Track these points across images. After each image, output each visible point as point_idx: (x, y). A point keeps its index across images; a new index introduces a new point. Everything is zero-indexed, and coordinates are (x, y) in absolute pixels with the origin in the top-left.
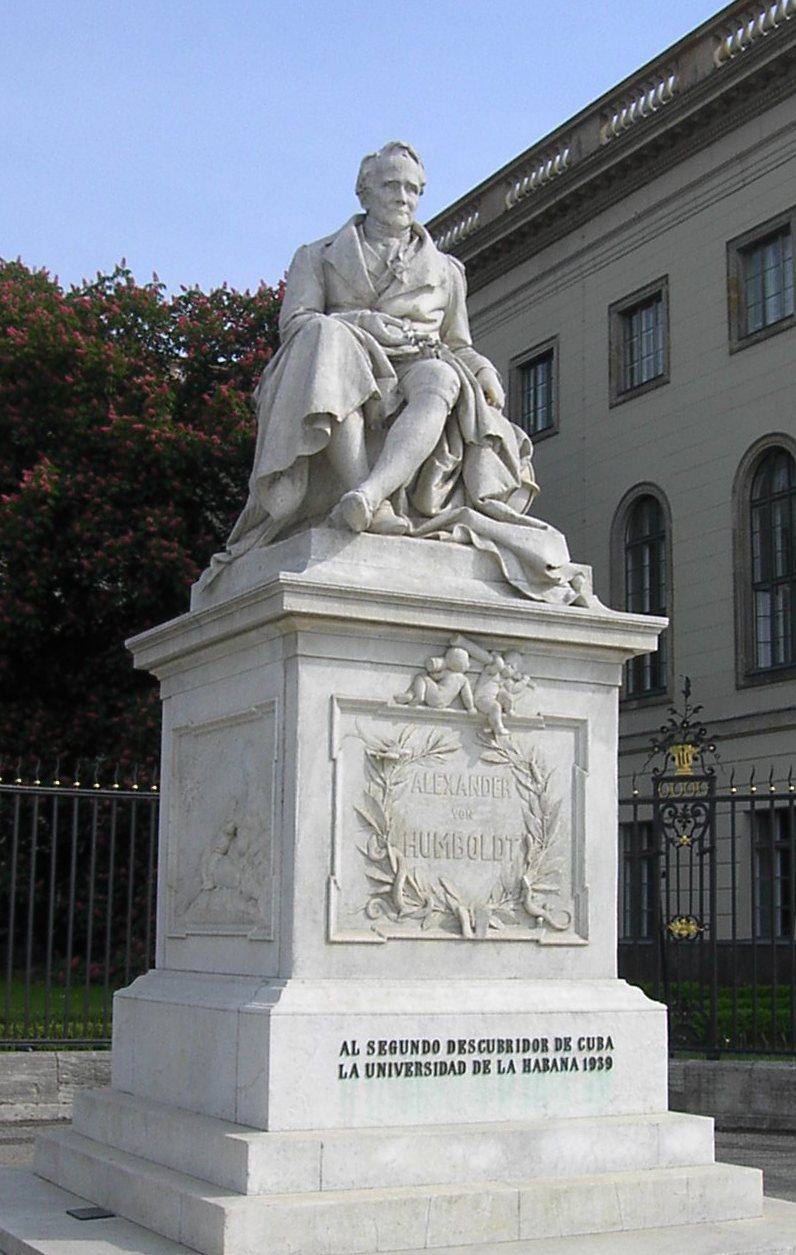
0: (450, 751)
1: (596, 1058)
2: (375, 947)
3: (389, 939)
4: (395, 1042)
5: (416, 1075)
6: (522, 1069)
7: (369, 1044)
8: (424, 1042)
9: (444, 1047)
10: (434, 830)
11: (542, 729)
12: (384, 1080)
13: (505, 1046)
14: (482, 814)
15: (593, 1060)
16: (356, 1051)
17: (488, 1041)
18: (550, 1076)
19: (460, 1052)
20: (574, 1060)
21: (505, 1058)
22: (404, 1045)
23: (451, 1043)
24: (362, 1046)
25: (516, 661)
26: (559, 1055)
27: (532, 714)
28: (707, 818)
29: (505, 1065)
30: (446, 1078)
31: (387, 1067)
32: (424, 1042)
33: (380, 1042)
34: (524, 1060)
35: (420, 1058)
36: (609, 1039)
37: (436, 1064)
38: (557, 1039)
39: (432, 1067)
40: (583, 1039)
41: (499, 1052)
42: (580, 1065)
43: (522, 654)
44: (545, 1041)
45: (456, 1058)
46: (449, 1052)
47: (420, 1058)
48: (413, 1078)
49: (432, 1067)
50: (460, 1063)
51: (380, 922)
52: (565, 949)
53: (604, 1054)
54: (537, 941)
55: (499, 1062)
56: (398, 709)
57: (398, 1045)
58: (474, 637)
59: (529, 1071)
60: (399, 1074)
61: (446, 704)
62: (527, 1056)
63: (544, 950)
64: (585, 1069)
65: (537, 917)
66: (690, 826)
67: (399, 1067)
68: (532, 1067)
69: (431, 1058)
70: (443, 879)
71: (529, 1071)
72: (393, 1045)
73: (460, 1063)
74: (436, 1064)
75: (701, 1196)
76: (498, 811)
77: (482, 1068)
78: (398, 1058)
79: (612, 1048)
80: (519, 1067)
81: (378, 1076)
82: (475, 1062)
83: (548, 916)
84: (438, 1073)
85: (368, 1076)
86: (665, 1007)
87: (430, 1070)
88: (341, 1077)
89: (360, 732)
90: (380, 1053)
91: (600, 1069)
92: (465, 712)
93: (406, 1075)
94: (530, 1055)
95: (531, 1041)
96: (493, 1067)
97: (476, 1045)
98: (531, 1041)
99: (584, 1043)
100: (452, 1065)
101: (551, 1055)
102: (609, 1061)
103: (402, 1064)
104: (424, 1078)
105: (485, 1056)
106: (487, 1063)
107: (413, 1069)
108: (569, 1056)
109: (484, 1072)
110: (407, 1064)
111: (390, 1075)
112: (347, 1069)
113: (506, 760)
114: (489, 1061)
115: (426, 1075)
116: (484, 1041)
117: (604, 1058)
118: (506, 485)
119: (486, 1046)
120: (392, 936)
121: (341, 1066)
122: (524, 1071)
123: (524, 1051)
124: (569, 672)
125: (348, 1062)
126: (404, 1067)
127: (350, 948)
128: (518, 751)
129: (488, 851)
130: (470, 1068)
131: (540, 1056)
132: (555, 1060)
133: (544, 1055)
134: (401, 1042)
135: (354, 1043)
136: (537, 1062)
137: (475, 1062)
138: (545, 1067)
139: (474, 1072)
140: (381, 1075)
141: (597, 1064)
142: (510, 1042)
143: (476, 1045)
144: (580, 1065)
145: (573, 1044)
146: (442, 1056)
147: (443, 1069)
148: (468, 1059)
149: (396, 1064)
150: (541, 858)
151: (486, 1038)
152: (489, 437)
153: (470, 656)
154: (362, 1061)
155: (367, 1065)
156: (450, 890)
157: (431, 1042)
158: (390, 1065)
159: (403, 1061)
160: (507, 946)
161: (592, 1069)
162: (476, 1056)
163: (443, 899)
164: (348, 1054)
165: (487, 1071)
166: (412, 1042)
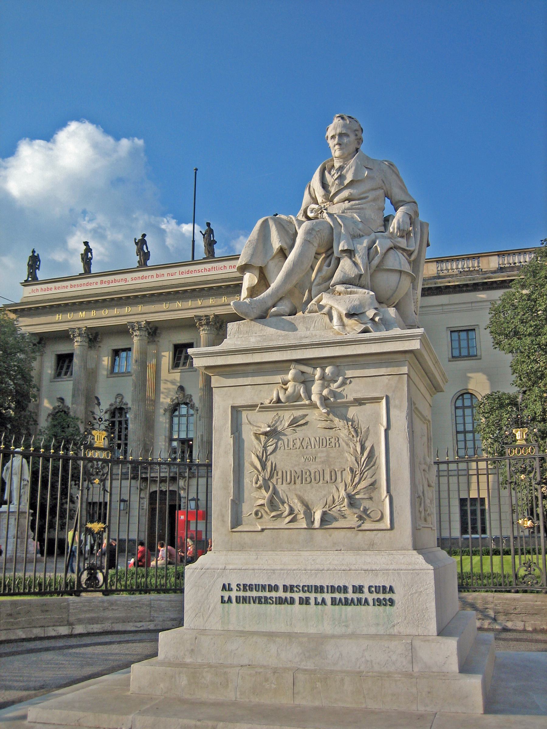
1: (382, 598)
4: (252, 585)
7: (237, 585)
9: (281, 588)
12: (247, 605)
13: (320, 589)
14: (320, 458)
15: (378, 599)
16: (230, 589)
17: (308, 586)
21: (320, 597)
24: (234, 587)
26: (355, 596)
29: (320, 600)
31: (248, 598)
32: (269, 585)
33: (244, 585)
34: (332, 598)
35: (268, 594)
36: (391, 587)
37: (276, 598)
38: (353, 586)
40: (372, 586)
42: (371, 602)
45: (288, 595)
46: (284, 592)
47: (268, 594)
48: (263, 606)
49: (274, 600)
50: (291, 598)
51: (260, 520)
53: (388, 596)
58: (305, 362)
62: (334, 595)
64: (374, 605)
71: (335, 605)
75: (429, 693)
76: (331, 455)
77: (305, 602)
78: (254, 594)
79: (393, 592)
80: (329, 601)
81: (243, 603)
82: (300, 598)
86: (432, 567)
88: (222, 602)
94: (337, 595)
96: (312, 601)
99: (373, 589)
101: (350, 595)
102: (392, 602)
104: (269, 605)
105: (307, 595)
106: (308, 599)
107: (263, 600)
108: (363, 596)
110: (259, 597)
111: (249, 603)
112: (226, 599)
116: (305, 586)
120: (264, 527)
122: (332, 604)
125: (226, 595)
129: (327, 477)
131: (342, 596)
135: (229, 584)
137: (300, 598)
138: (347, 602)
139: (300, 604)
142: (322, 587)
143: (301, 588)
144: (371, 602)
145: (366, 590)
146: (281, 594)
147: (281, 601)
148: (296, 596)
150: (357, 480)
154: (234, 594)
155: (236, 597)
157: (273, 585)
159: (258, 595)
160: (336, 532)
166: (262, 585)
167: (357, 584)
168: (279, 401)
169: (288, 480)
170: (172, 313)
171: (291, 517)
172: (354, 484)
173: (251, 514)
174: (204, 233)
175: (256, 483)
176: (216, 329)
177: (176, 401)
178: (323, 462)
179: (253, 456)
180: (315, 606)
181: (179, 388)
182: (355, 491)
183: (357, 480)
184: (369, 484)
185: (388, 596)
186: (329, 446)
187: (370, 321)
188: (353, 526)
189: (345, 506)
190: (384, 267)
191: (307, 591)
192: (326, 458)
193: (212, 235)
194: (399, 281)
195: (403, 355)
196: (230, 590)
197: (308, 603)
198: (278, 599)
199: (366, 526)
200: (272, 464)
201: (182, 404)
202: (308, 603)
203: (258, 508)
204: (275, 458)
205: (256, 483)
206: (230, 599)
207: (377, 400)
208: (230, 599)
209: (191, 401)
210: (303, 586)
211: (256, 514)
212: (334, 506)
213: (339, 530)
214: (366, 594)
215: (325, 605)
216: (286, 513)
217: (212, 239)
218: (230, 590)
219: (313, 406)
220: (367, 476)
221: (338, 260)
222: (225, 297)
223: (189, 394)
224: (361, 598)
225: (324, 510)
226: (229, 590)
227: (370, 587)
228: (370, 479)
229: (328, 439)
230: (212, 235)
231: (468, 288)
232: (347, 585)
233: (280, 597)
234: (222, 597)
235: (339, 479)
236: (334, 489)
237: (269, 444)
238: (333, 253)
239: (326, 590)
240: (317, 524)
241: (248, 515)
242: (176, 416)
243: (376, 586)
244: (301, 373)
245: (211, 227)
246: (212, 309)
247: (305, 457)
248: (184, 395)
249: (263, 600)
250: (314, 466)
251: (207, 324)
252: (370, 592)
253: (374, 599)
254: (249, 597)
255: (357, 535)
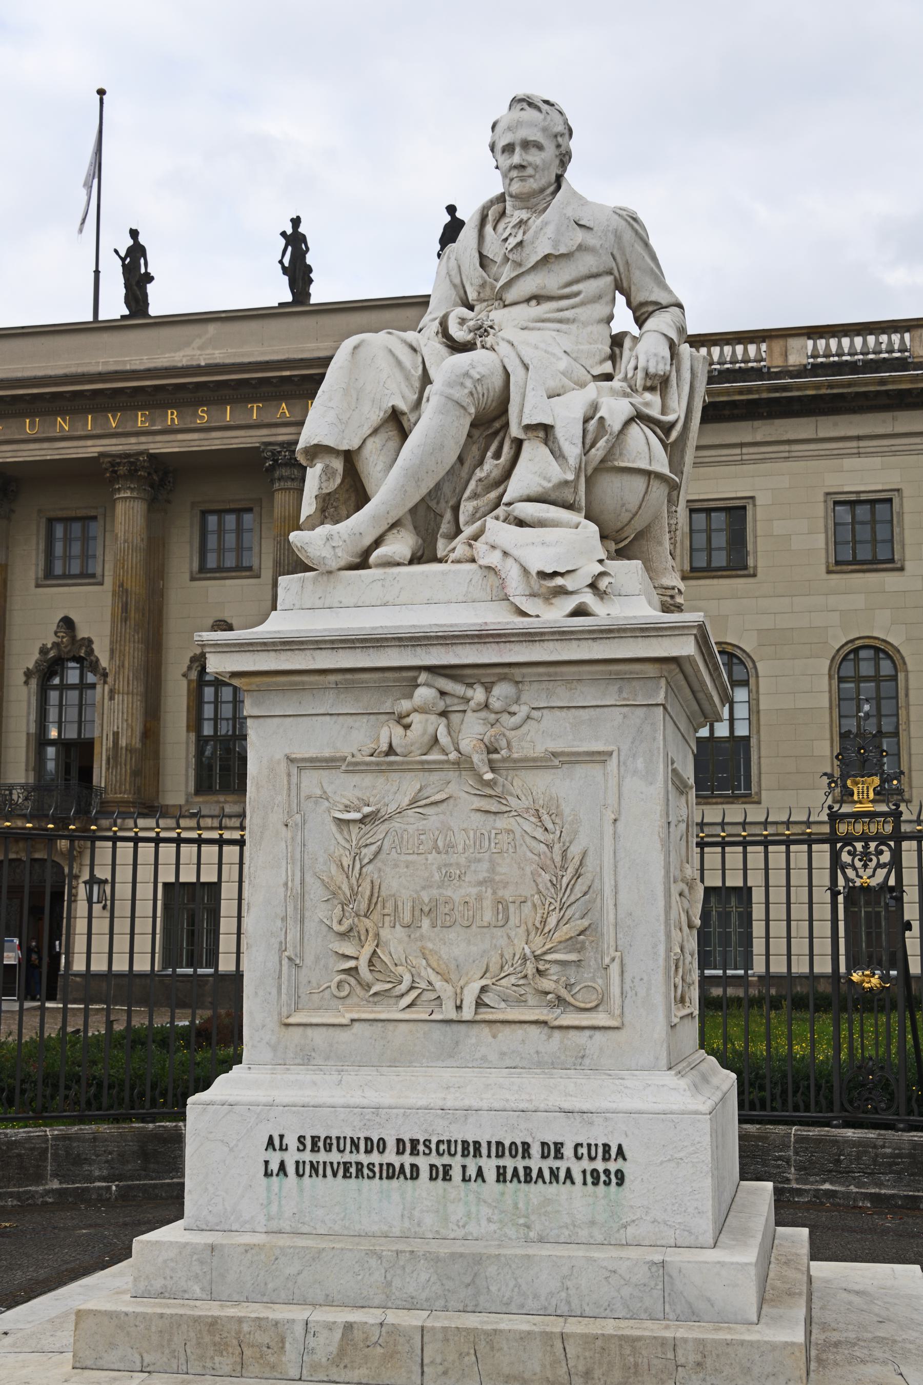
0: (432, 804)
1: (601, 1170)
2: (338, 1031)
3: (353, 1020)
4: (331, 1138)
5: (357, 1177)
6: (494, 1177)
8: (367, 1139)
10: (415, 896)
11: (556, 767)
13: (472, 1149)
16: (284, 1147)
17: (449, 1142)
18: (536, 1191)
19: (412, 1154)
20: (568, 1171)
22: (342, 1141)
23: (399, 1141)
24: (291, 1141)
25: (502, 690)
26: (546, 1165)
27: (539, 750)
28: (892, 856)
29: (472, 1171)
30: (395, 1183)
32: (367, 1139)
33: (313, 1138)
34: (498, 1167)
36: (620, 1147)
38: (543, 1144)
39: (377, 1169)
40: (581, 1145)
41: (463, 1155)
43: (517, 683)
44: (526, 1146)
45: (408, 1159)
46: (398, 1153)
48: (353, 1180)
49: (377, 1169)
50: (413, 1166)
51: (349, 1001)
52: (587, 1033)
53: (613, 1166)
54: (545, 1023)
55: (464, 1167)
56: (367, 764)
57: (334, 1142)
58: (448, 672)
59: (505, 1181)
60: (335, 1175)
61: (419, 752)
62: (501, 1162)
63: (557, 1034)
64: (585, 1183)
65: (547, 993)
66: (873, 864)
67: (335, 1166)
68: (509, 1176)
69: (375, 1158)
70: (427, 952)
72: (328, 1141)
73: (413, 1166)
74: (381, 1165)
78: (335, 1157)
79: (625, 1159)
80: (490, 1174)
81: (311, 1176)
82: (432, 1166)
83: (564, 993)
84: (384, 1175)
85: (299, 1175)
87: (374, 1173)
89: (325, 792)
90: (312, 1150)
91: (607, 1184)
92: (444, 757)
93: (345, 1176)
94: (509, 1163)
95: (507, 1145)
96: (456, 1173)
97: (433, 1146)
98: (507, 1145)
99: (583, 1151)
100: (402, 1166)
101: (535, 1163)
103: (339, 1163)
104: (366, 1180)
105: (446, 1160)
106: (447, 1168)
107: (353, 1170)
108: (562, 1165)
109: (444, 1179)
110: (345, 1163)
111: (325, 1176)
112: (274, 1166)
113: (508, 809)
114: (450, 1166)
115: (369, 1177)
116: (443, 1141)
117: (613, 1171)
118: (549, 481)
119: (447, 1147)
121: (267, 1163)
122: (498, 1181)
123: (497, 1156)
124: (588, 695)
126: (342, 1166)
127: (309, 1031)
128: (523, 798)
129: (488, 916)
130: (424, 1173)
131: (520, 1164)
132: (540, 1170)
133: (527, 1162)
134: (338, 1138)
135: (282, 1137)
136: (515, 1169)
137: (432, 1166)
139: (431, 1179)
140: (314, 1175)
141: (603, 1178)
142: (477, 1144)
143: (433, 1146)
144: (578, 1177)
145: (568, 1151)
146: (391, 1157)
147: (391, 1172)
148: (423, 1163)
149: (331, 1163)
150: (552, 921)
151: (445, 1138)
152: (528, 428)
153: (443, 693)
154: (291, 1158)
155: (297, 1163)
156: (435, 965)
158: (325, 1163)
161: (595, 1183)
162: (434, 1159)
163: (423, 973)
164: (274, 1150)
165: (447, 1177)
166: (352, 1139)
167: (550, 1139)
168: (391, 751)
169: (407, 918)
170: (45, 445)
171: (414, 994)
172: (546, 930)
173: (329, 987)
174: (123, 254)
175: (340, 922)
176: (152, 486)
177: (52, 654)
178: (480, 883)
179: (334, 869)
180: (462, 1185)
181: (61, 623)
182: (547, 946)
183: (552, 921)
184: (578, 932)
185: (613, 1166)
186: (495, 851)
187: (588, 590)
188: (542, 1018)
189: (525, 977)
190: (616, 463)
191: (446, 1152)
192: (486, 875)
193: (142, 261)
194: (646, 493)
195: (657, 666)
196: (283, 1149)
197: (448, 1178)
198: (385, 1167)
199: (570, 1019)
200: (372, 882)
201: (69, 660)
202: (448, 1178)
203: (343, 976)
204: (380, 870)
205: (340, 922)
206: (282, 1167)
207: (600, 757)
208: (282, 1167)
209: (91, 652)
210: (439, 1142)
211: (339, 985)
212: (503, 975)
213: (513, 1026)
214: (568, 1161)
215: (484, 1181)
216: (403, 987)
217: (143, 271)
218: (283, 1149)
219: (463, 764)
220: (573, 915)
221: (518, 444)
222: (172, 414)
223: (86, 636)
224: (558, 1169)
225: (484, 982)
226: (281, 1149)
227: (577, 1146)
228: (579, 922)
229: (493, 835)
230: (142, 261)
231: (736, 412)
232: (529, 1140)
233: (389, 1165)
234: (267, 1163)
235: (514, 920)
236: (503, 942)
237: (368, 842)
238: (507, 425)
239: (484, 1151)
240: (468, 1013)
241: (321, 989)
242: (55, 687)
243: (589, 1145)
244: (439, 695)
245: (142, 240)
246: (143, 439)
247: (444, 872)
248: (73, 638)
249: (353, 1170)
250: (462, 892)
251: (132, 474)
252: (578, 1157)
253: (584, 1172)
254: (325, 1163)
255: (550, 1037)
